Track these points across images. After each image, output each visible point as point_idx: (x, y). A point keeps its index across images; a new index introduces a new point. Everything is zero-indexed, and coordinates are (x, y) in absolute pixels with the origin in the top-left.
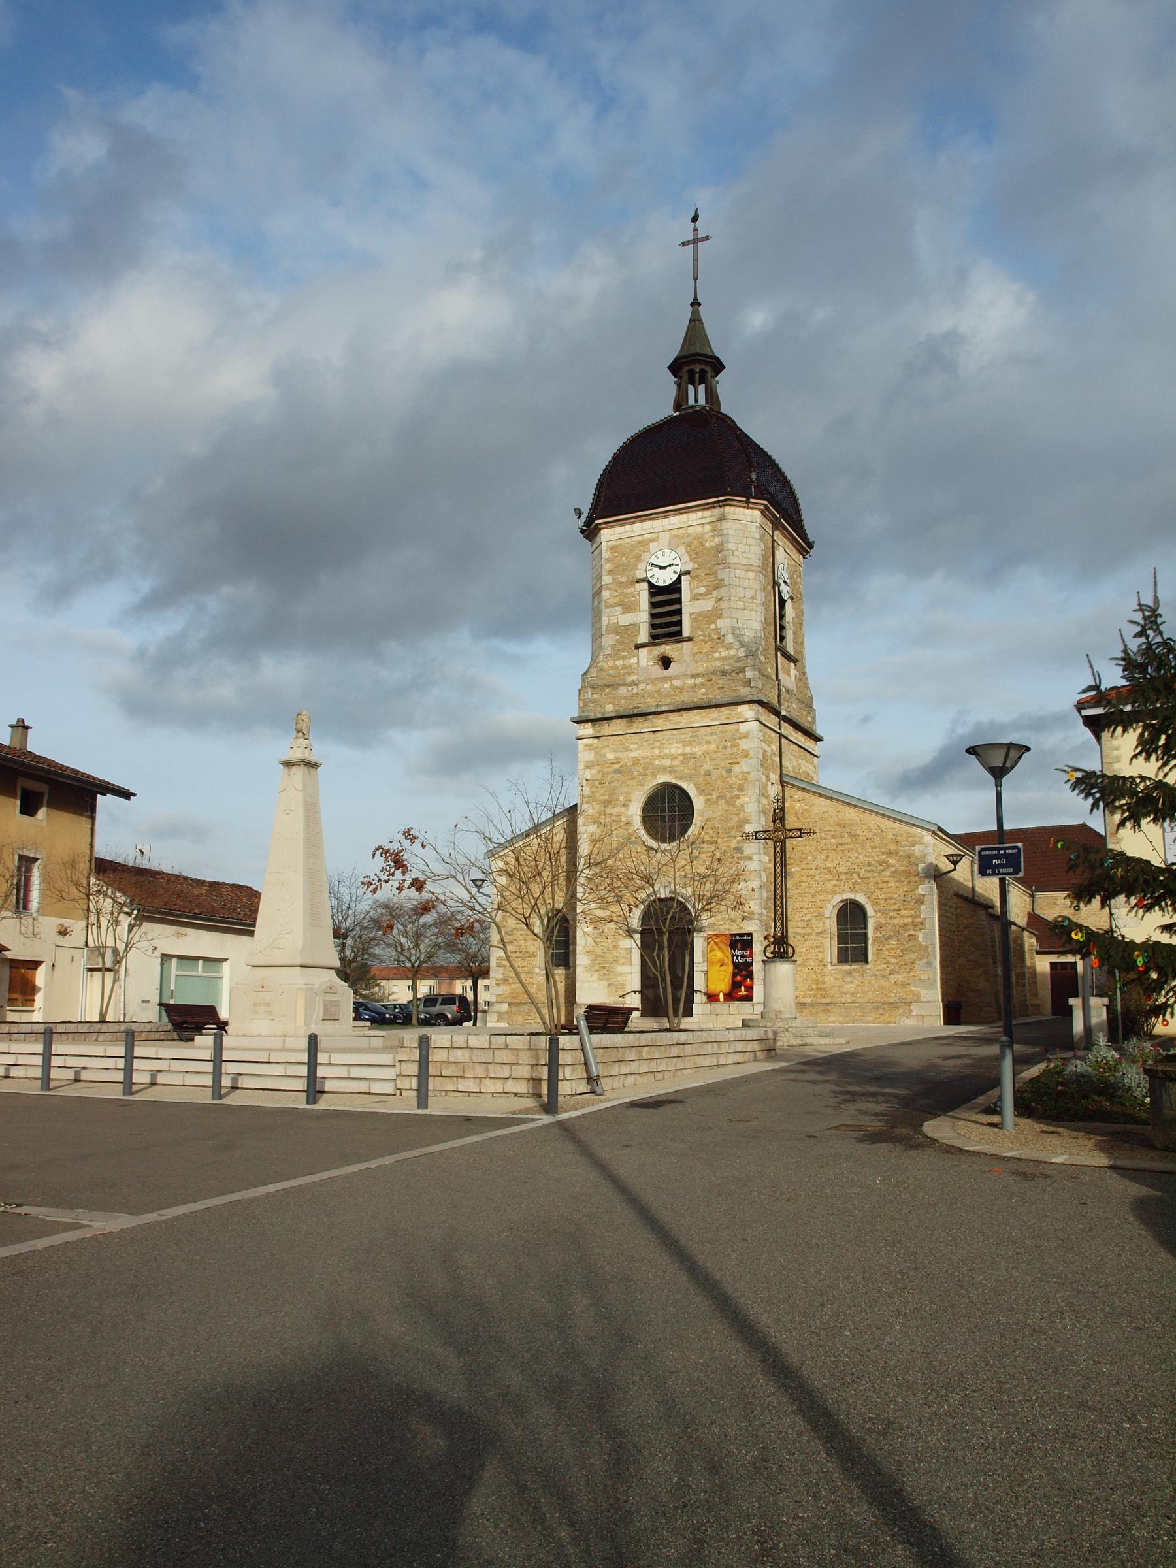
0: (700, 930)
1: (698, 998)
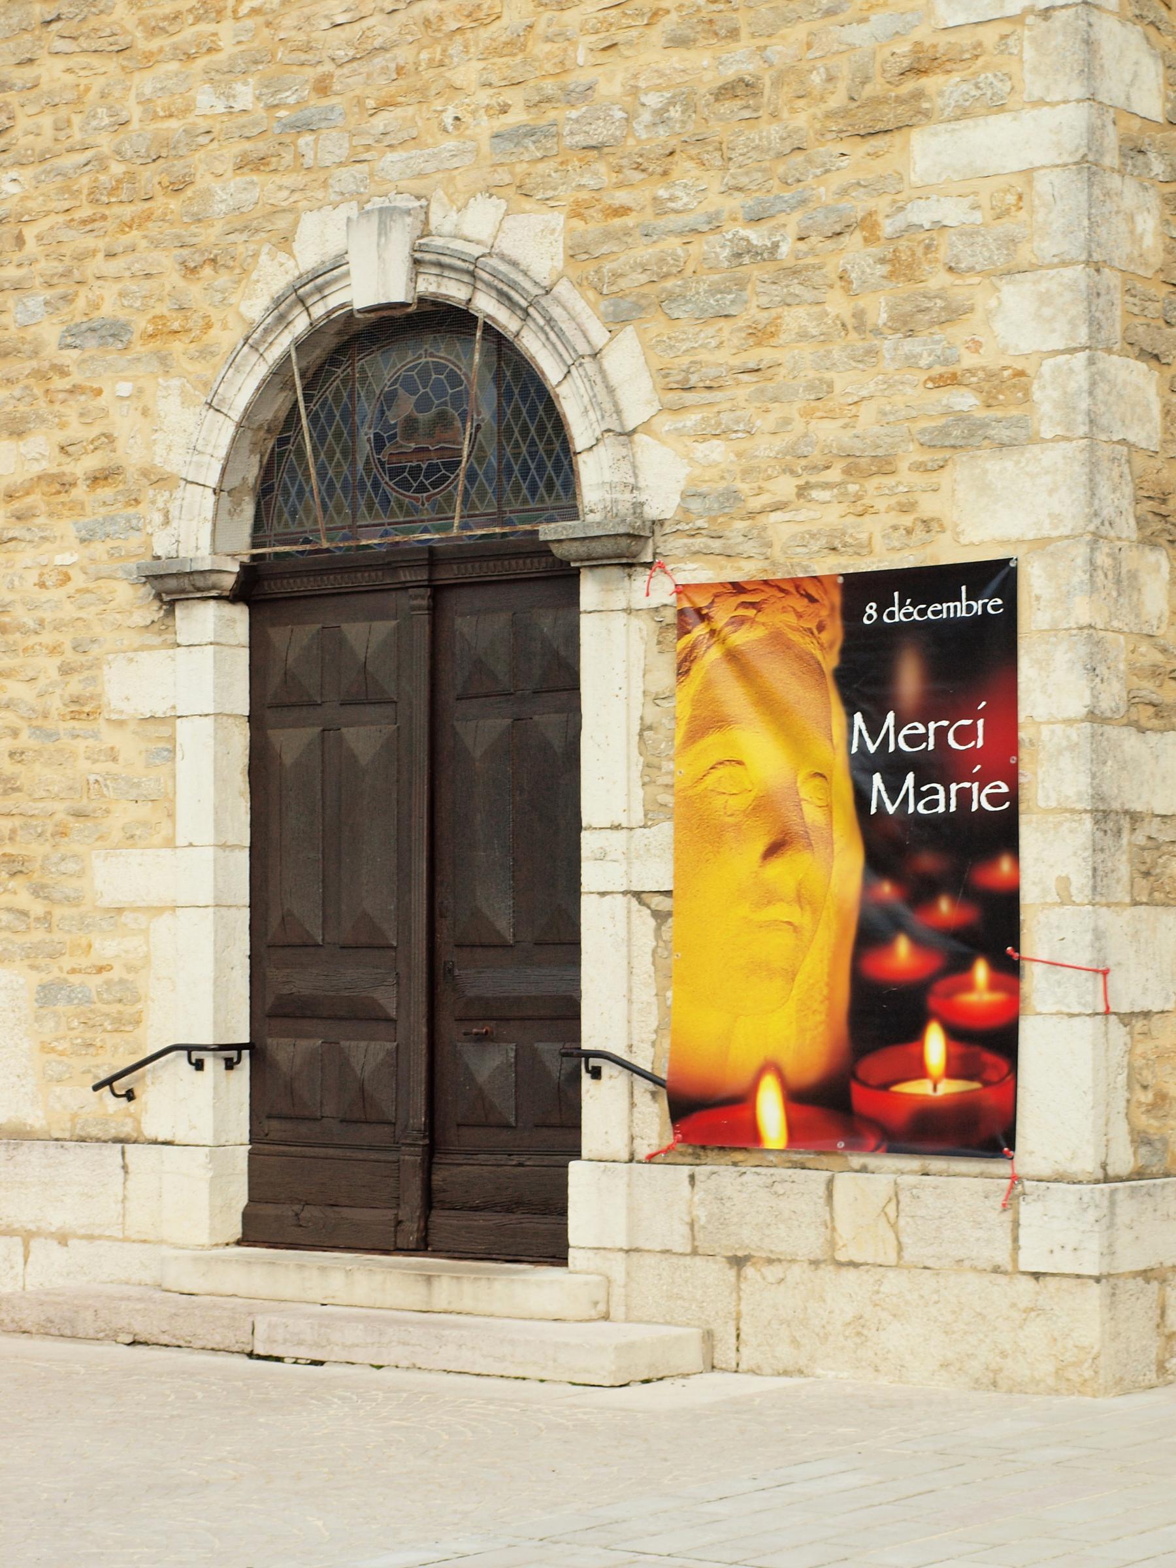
0: (627, 551)
1: (611, 1114)
